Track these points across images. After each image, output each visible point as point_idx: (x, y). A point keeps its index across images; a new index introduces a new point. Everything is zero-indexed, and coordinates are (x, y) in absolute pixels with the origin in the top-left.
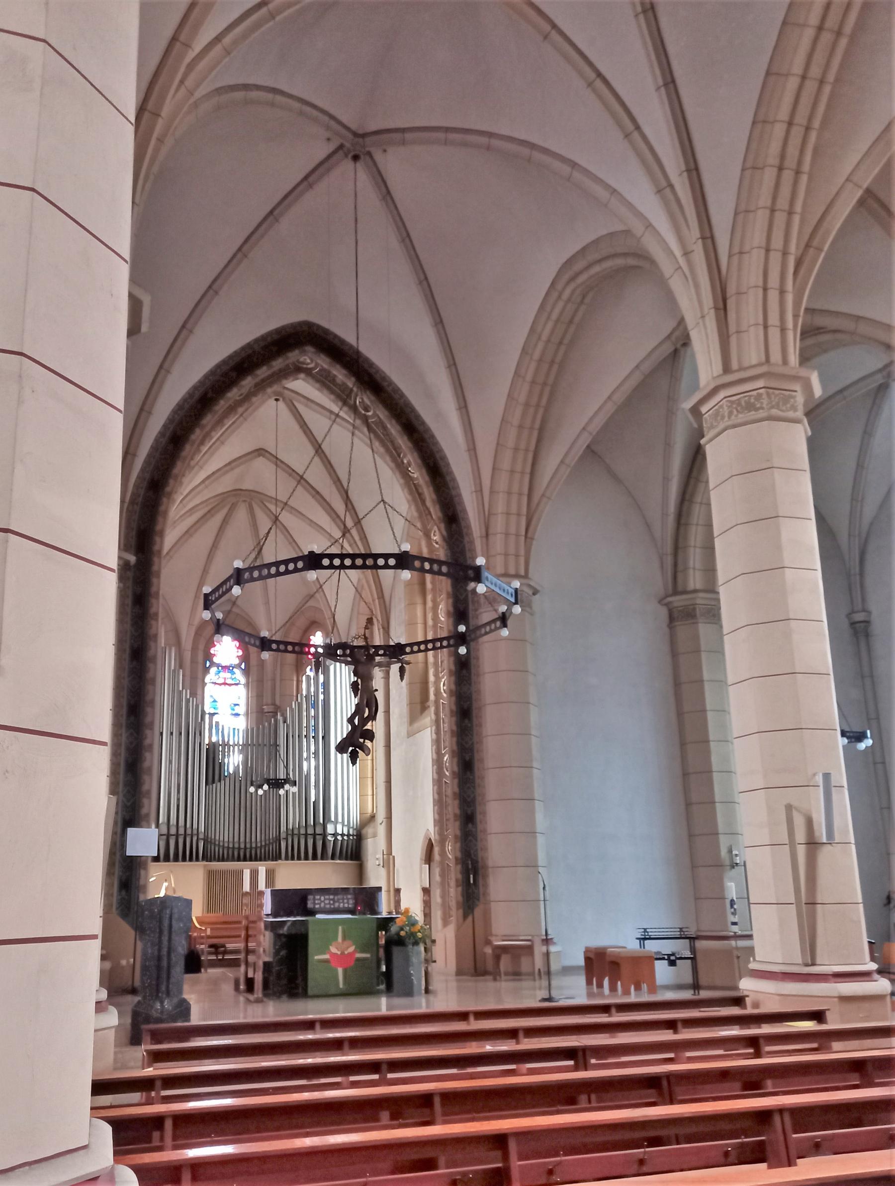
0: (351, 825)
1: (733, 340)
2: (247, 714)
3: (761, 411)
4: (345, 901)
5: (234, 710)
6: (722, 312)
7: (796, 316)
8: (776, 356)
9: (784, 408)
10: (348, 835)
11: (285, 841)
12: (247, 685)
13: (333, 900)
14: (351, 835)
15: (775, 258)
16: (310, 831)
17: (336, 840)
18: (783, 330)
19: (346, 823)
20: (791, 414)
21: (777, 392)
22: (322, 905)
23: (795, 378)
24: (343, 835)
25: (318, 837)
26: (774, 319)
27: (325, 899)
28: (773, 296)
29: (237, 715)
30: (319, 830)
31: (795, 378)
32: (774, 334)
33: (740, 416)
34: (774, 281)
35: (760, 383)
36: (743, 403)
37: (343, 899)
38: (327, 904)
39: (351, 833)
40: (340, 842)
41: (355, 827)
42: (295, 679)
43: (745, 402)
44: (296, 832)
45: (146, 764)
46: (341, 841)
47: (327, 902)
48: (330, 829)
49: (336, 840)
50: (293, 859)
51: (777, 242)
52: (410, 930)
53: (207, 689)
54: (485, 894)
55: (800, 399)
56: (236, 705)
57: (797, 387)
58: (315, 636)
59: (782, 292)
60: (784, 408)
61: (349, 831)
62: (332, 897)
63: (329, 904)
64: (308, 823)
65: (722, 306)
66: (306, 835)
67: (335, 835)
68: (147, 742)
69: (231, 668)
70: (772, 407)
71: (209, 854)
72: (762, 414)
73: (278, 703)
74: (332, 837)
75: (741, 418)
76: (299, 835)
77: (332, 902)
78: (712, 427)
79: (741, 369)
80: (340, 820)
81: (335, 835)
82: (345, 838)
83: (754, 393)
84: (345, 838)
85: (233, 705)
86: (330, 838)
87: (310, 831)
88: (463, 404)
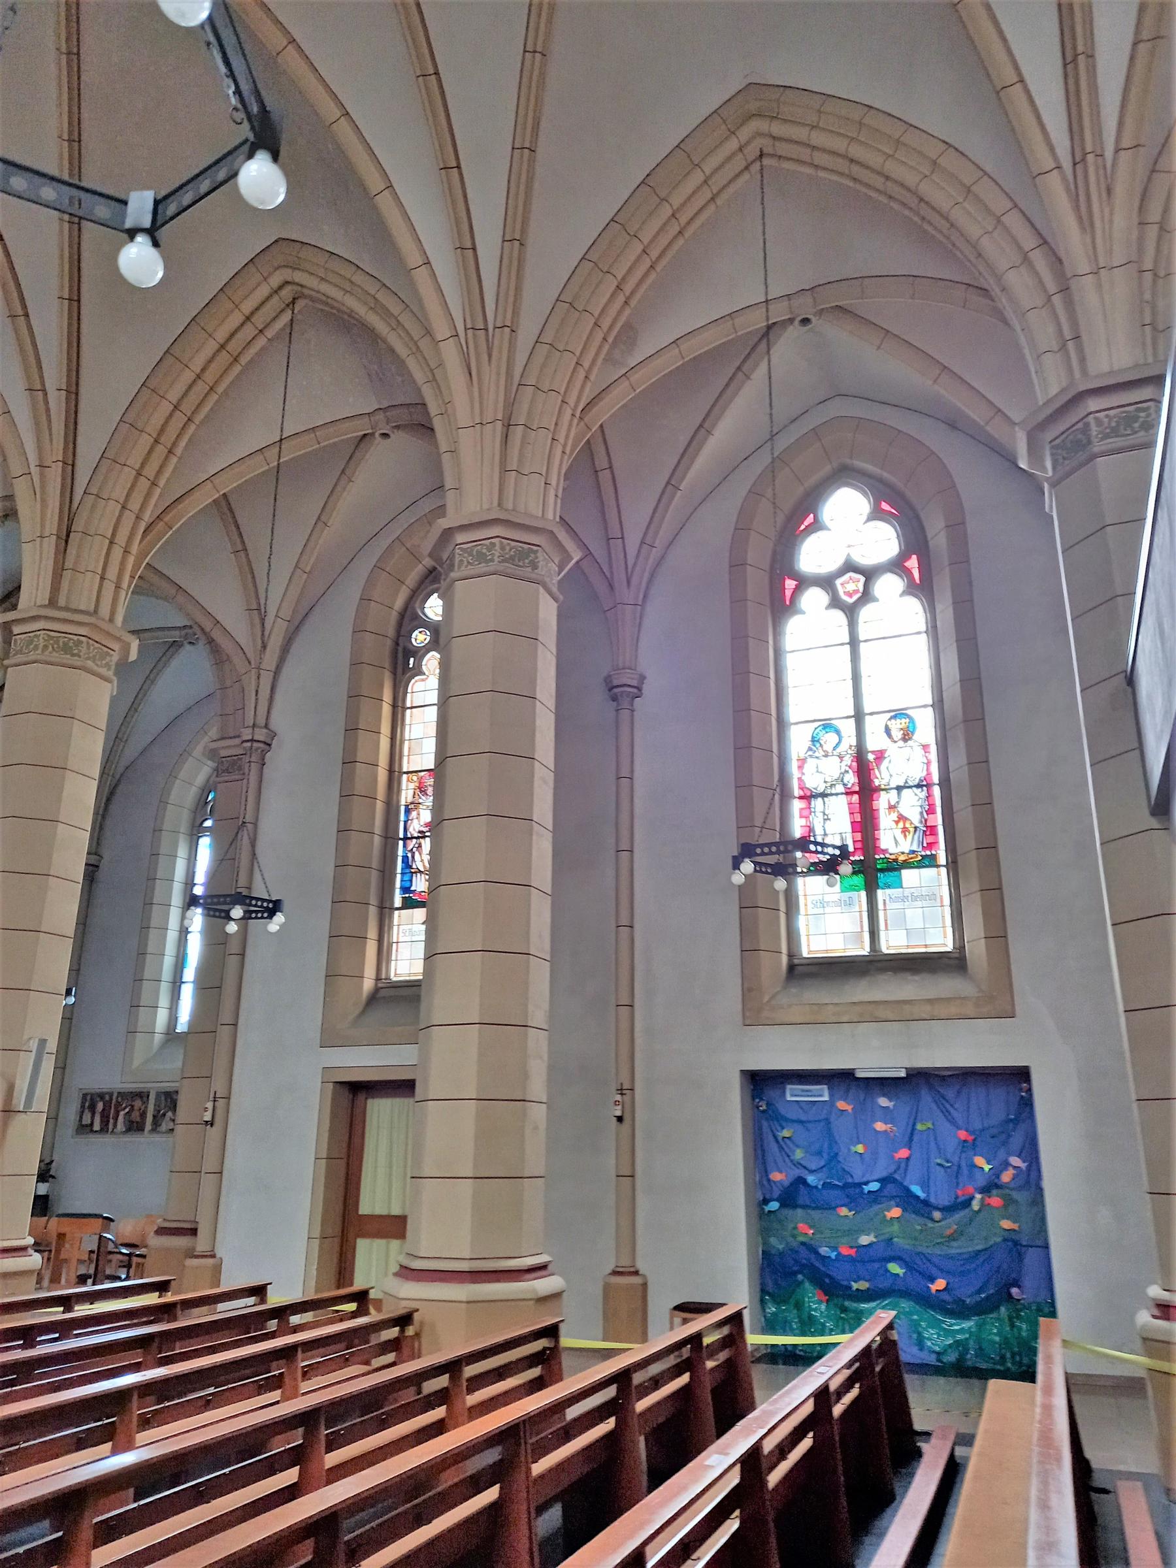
1: (67, 574)
3: (76, 658)
7: (132, 577)
8: (105, 610)
9: (99, 663)
15: (128, 519)
18: (118, 587)
20: (103, 671)
21: (97, 645)
23: (118, 639)
26: (112, 574)
28: (117, 552)
31: (118, 639)
32: (109, 588)
33: (54, 654)
34: (121, 538)
35: (82, 631)
36: (61, 644)
43: (64, 642)
51: (135, 505)
55: (115, 657)
57: (116, 646)
59: (126, 551)
60: (99, 663)
65: (65, 537)
70: (88, 659)
72: (76, 661)
75: (56, 657)
78: (20, 652)
79: (67, 609)
83: (76, 638)
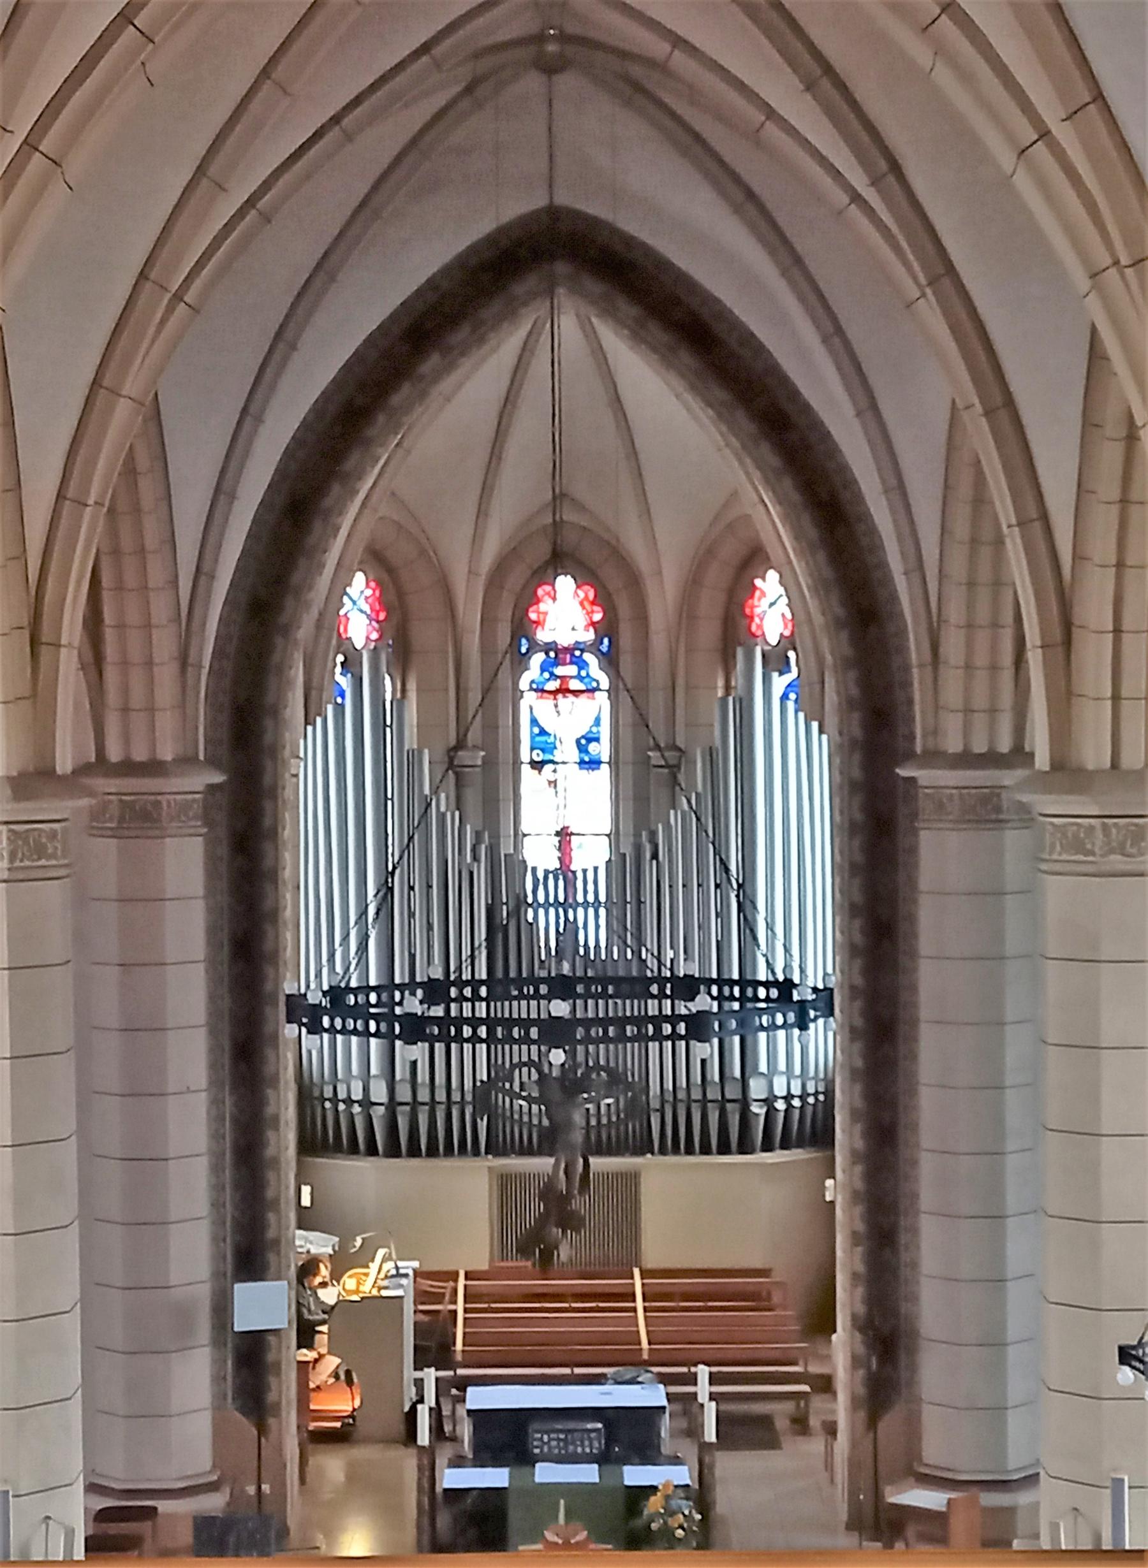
0: (812, 1073)
2: (614, 763)
4: (587, 1443)
5: (587, 752)
6: (1060, 650)
10: (803, 1097)
11: (658, 1114)
12: (612, 692)
13: (565, 1440)
14: (809, 1095)
16: (713, 1093)
17: (771, 1112)
19: (797, 1070)
22: (546, 1449)
24: (788, 1098)
25: (729, 1106)
27: (550, 1440)
29: (592, 764)
30: (732, 1092)
37: (582, 1442)
38: (555, 1447)
39: (811, 1089)
40: (781, 1115)
41: (822, 1075)
42: (721, 683)
44: (681, 1095)
45: (270, 1152)
46: (786, 1111)
47: (554, 1443)
48: (757, 1089)
49: (771, 1112)
50: (676, 1150)
52: (665, 1523)
53: (524, 705)
54: (912, 1383)
56: (590, 740)
58: (764, 579)
61: (804, 1086)
62: (562, 1436)
63: (558, 1446)
64: (709, 1077)
66: (704, 1101)
67: (769, 1101)
68: (270, 1110)
69: (577, 653)
71: (501, 1139)
73: (680, 742)
74: (761, 1107)
76: (689, 1100)
77: (562, 1444)
80: (782, 1066)
81: (769, 1101)
82: (796, 1103)
84: (796, 1103)
85: (583, 742)
86: (756, 1108)
87: (713, 1093)
88: (864, 403)
